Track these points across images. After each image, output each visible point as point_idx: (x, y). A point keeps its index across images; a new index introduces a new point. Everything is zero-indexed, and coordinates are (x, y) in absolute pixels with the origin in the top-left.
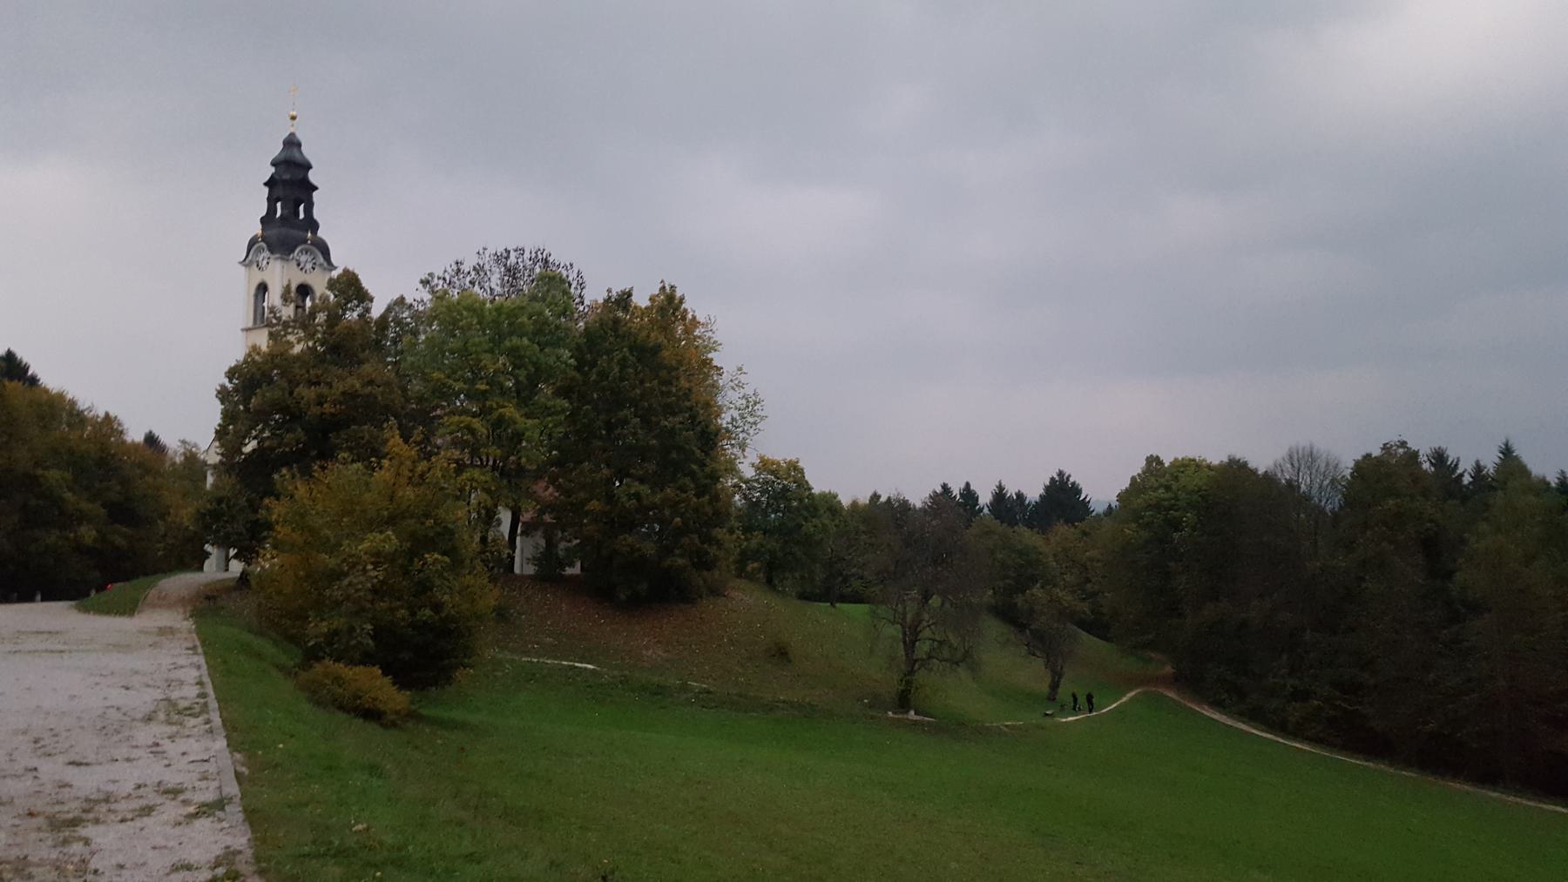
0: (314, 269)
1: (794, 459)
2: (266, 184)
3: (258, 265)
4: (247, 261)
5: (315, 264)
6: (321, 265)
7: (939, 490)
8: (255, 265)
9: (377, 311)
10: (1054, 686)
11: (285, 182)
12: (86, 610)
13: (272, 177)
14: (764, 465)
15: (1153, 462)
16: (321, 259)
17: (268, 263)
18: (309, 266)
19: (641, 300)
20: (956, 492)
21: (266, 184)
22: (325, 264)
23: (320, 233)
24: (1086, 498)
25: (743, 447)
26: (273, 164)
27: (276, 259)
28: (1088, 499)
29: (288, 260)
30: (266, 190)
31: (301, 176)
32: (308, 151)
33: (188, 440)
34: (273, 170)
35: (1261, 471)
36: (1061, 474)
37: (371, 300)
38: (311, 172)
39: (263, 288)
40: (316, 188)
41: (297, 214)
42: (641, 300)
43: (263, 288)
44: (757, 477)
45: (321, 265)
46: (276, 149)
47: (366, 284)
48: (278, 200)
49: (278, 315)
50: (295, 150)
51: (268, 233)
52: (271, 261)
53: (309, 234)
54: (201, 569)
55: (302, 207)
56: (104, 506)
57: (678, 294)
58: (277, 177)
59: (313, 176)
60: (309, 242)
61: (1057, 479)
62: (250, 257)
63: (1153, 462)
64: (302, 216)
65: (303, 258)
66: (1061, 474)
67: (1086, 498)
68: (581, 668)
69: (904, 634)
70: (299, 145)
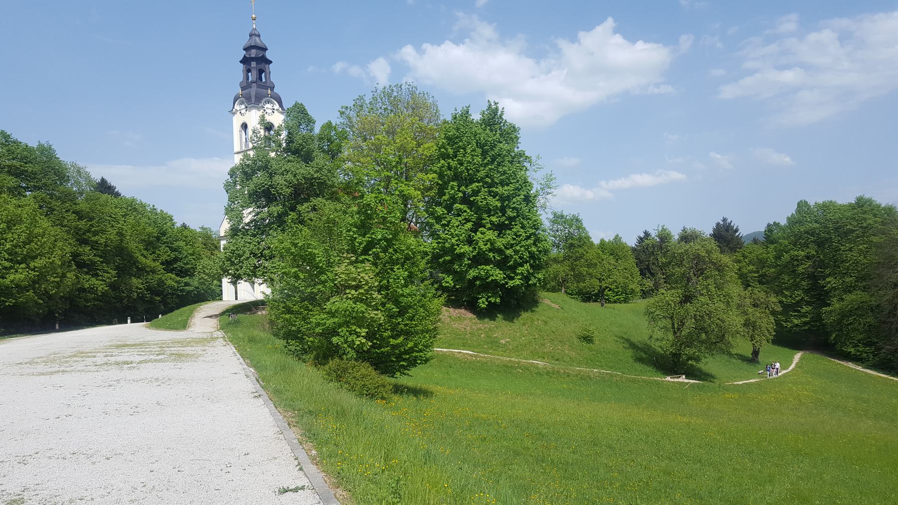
0: (273, 112)
1: (576, 213)
2: (241, 62)
3: (240, 112)
4: (234, 110)
5: (274, 109)
6: (277, 110)
7: (642, 235)
8: (239, 112)
9: (317, 130)
10: (756, 353)
11: (253, 59)
12: (158, 327)
13: (245, 56)
14: (558, 218)
15: (802, 206)
16: (277, 106)
17: (246, 111)
18: (269, 111)
19: (476, 117)
20: (653, 234)
21: (241, 62)
22: (280, 109)
23: (275, 90)
24: (739, 234)
25: (544, 207)
26: (244, 50)
27: (251, 107)
28: (740, 236)
29: (259, 109)
30: (242, 64)
31: (261, 55)
32: (265, 40)
33: (205, 227)
34: (245, 52)
35: (883, 206)
36: (724, 220)
37: (314, 123)
38: (267, 51)
39: (245, 126)
40: (271, 62)
41: (261, 79)
42: (476, 117)
43: (245, 126)
44: (551, 227)
45: (277, 110)
46: (245, 41)
47: (311, 112)
48: (249, 71)
49: (258, 135)
50: (257, 39)
51: (244, 92)
52: (248, 109)
53: (269, 91)
54: (221, 299)
55: (263, 75)
56: (162, 264)
57: (500, 109)
58: (248, 56)
59: (269, 55)
60: (269, 96)
61: (722, 223)
62: (235, 107)
63: (802, 206)
64: (264, 80)
65: (268, 106)
66: (724, 220)
67: (739, 234)
68: (469, 351)
69: (673, 324)
70: (259, 36)
